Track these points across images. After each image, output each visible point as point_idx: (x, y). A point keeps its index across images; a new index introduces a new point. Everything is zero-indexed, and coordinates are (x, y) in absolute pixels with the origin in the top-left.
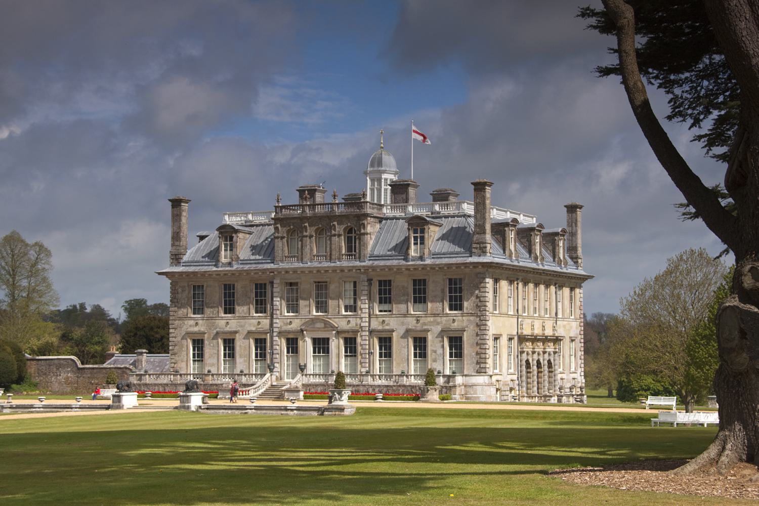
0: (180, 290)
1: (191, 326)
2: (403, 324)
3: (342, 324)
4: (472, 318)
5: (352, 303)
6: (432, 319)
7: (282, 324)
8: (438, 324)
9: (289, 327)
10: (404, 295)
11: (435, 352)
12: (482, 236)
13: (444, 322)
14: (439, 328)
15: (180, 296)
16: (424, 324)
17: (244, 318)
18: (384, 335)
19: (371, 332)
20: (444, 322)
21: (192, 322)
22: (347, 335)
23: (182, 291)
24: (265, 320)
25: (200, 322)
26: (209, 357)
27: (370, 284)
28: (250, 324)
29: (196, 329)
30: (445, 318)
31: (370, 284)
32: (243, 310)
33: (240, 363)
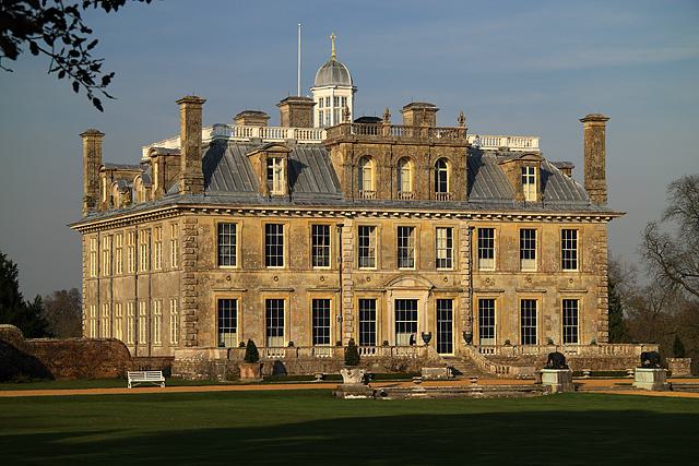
0: (200, 230)
1: (218, 281)
2: (510, 283)
3: (438, 282)
4: (591, 278)
5: (445, 256)
6: (544, 278)
7: (356, 281)
8: (553, 284)
9: (366, 284)
10: (511, 248)
11: (549, 318)
12: (602, 181)
13: (559, 283)
14: (554, 289)
15: (200, 238)
16: (536, 284)
17: (300, 271)
18: (488, 296)
19: (471, 291)
20: (559, 283)
21: (219, 275)
22: (442, 296)
23: (205, 231)
24: (330, 275)
25: (233, 275)
26: (248, 326)
27: (470, 234)
28: (308, 281)
29: (227, 285)
30: (560, 277)
31: (470, 234)
32: (297, 262)
33: (294, 333)
